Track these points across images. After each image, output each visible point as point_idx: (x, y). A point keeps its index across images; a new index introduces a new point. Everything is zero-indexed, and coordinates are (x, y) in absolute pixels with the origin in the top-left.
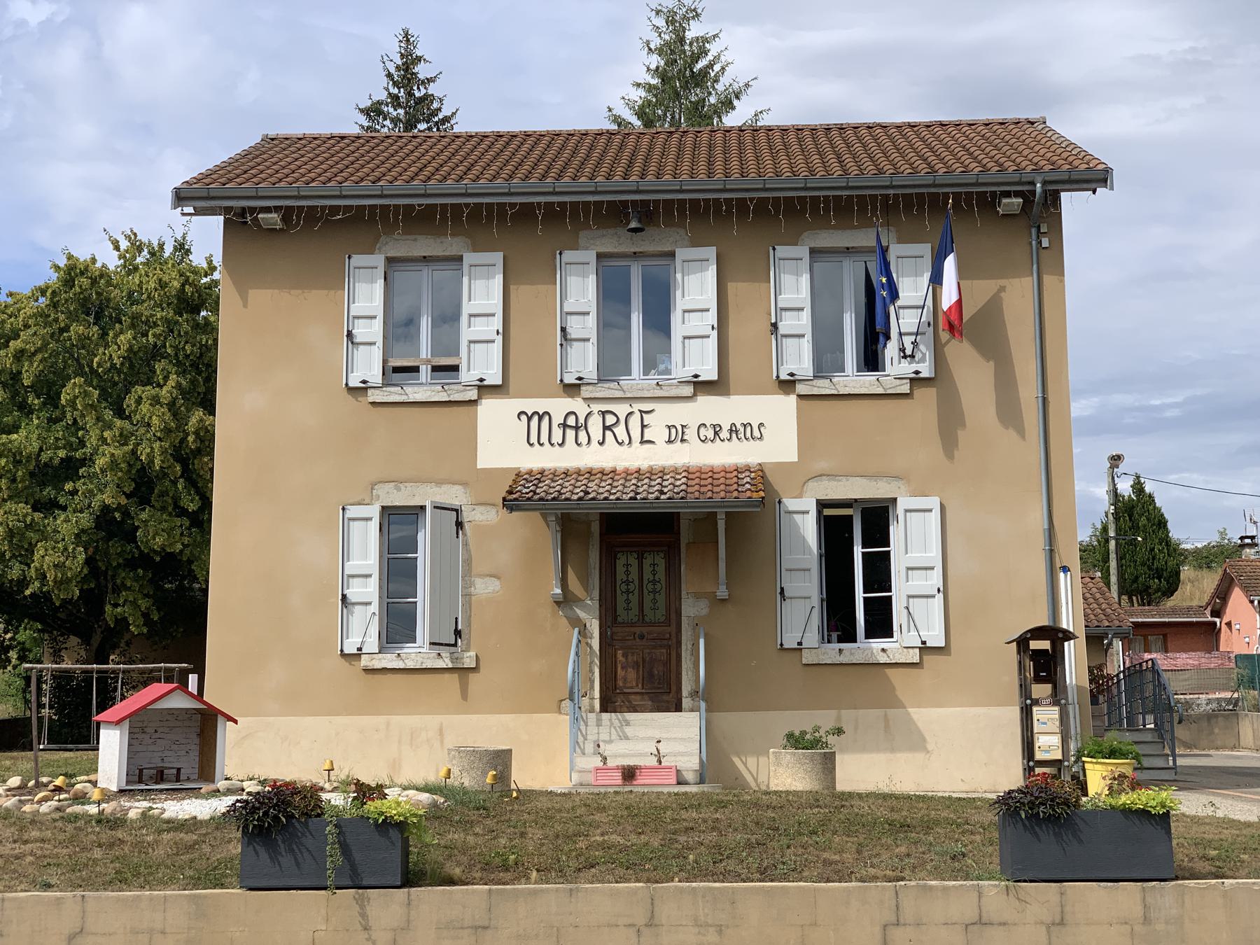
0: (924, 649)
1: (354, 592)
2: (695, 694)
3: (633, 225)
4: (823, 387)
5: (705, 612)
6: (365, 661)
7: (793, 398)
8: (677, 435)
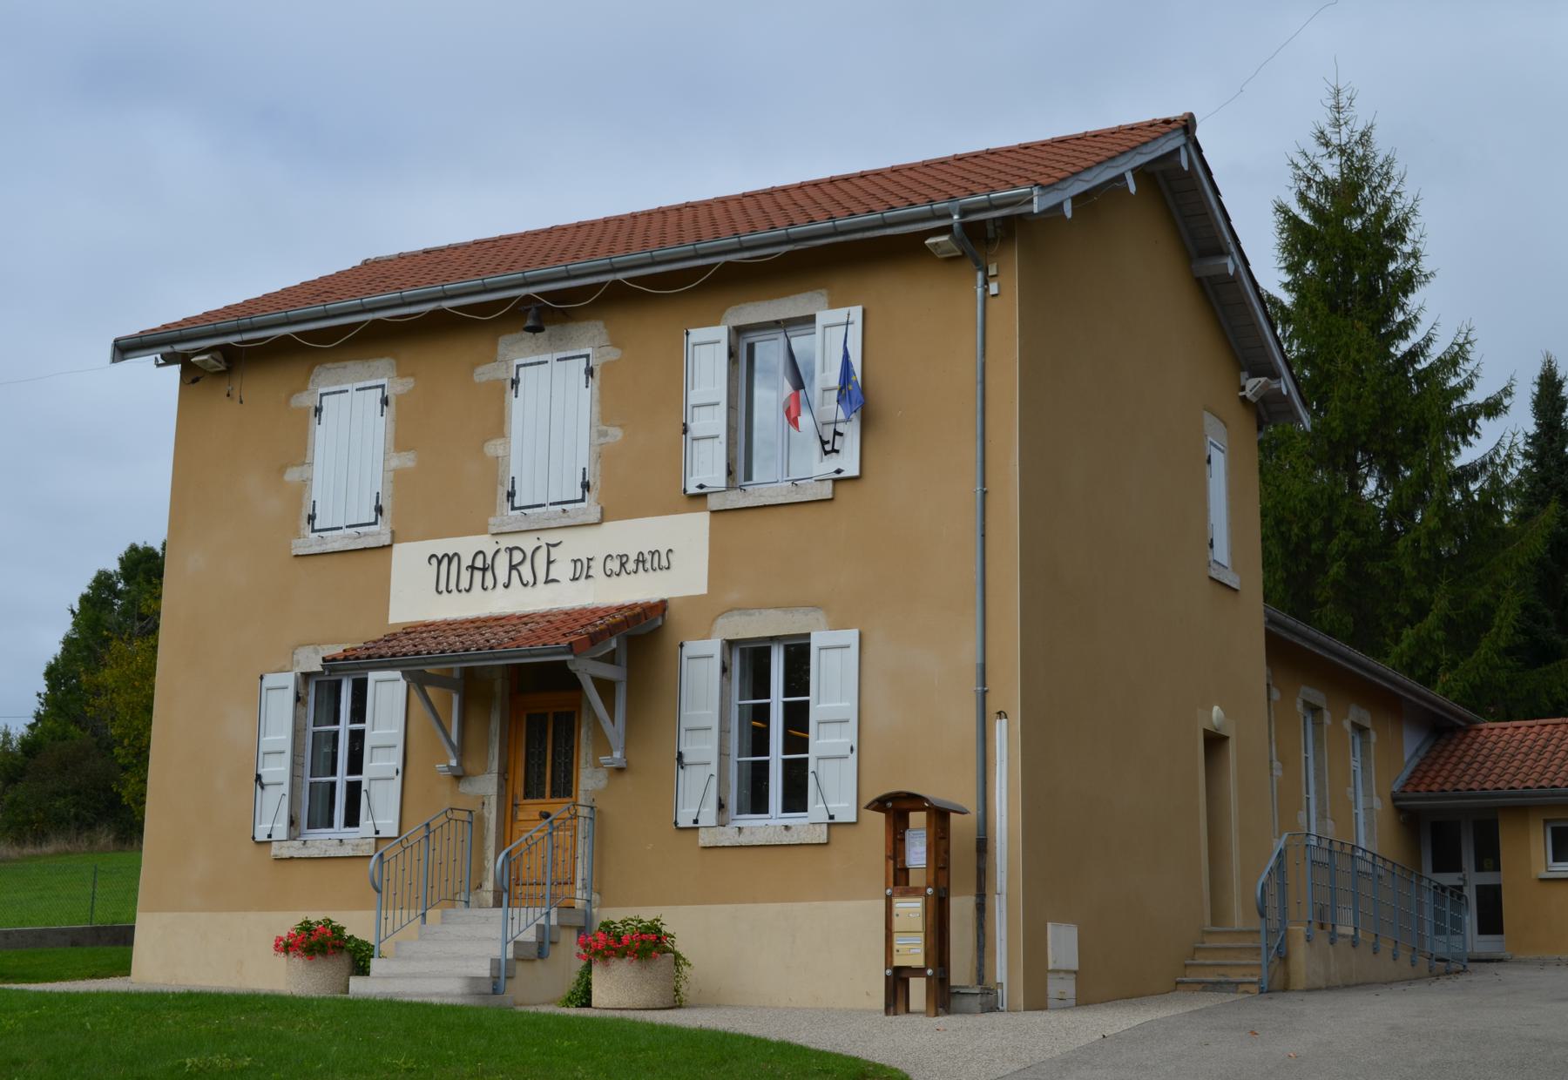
0: (832, 824)
3: (530, 323)
4: (736, 500)
5: (603, 783)
8: (582, 569)
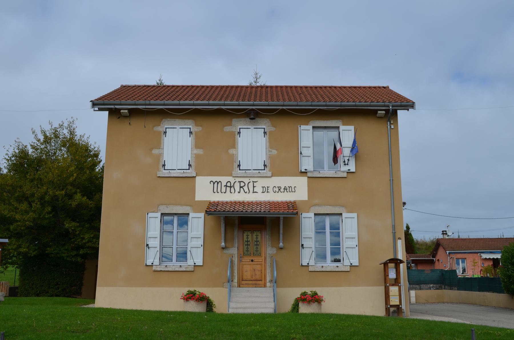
0: (351, 266)
1: (151, 243)
2: (271, 281)
3: (252, 117)
5: (275, 252)
6: (154, 268)
7: (306, 178)
8: (266, 190)
